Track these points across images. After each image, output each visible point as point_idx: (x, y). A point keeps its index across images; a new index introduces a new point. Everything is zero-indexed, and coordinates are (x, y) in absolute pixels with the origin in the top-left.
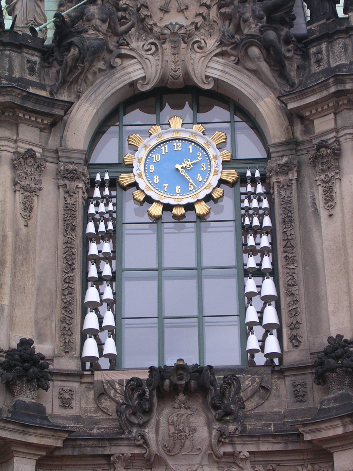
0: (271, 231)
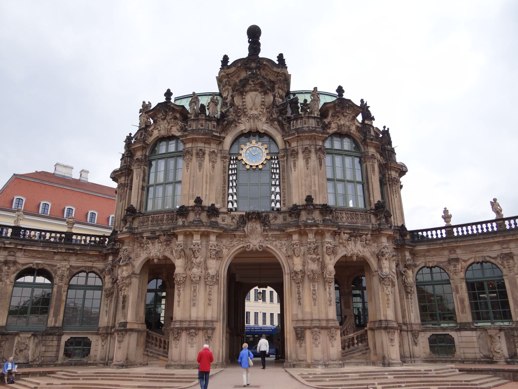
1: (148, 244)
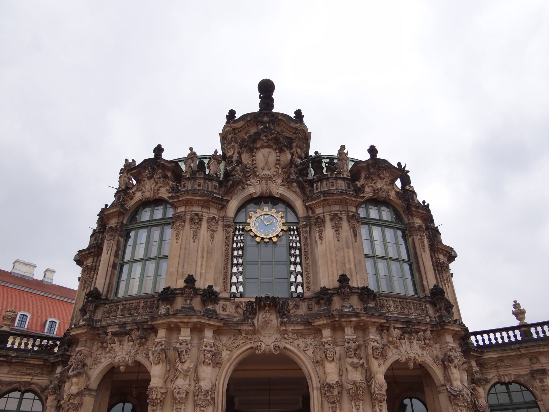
0: (300, 249)
1: (113, 343)
